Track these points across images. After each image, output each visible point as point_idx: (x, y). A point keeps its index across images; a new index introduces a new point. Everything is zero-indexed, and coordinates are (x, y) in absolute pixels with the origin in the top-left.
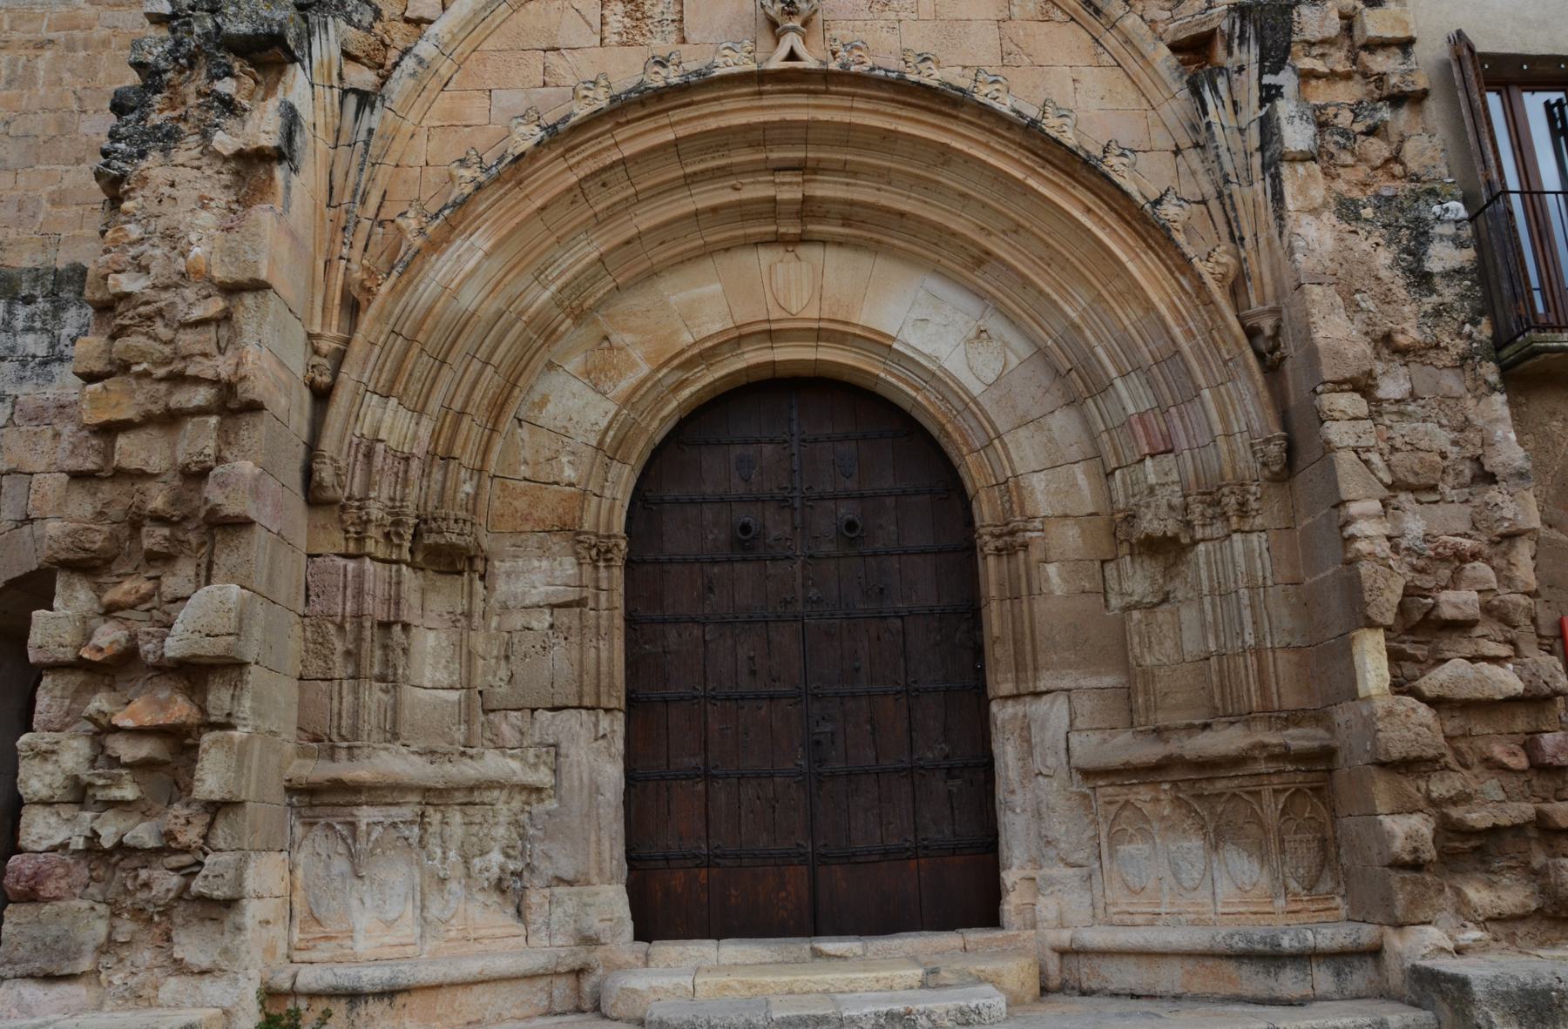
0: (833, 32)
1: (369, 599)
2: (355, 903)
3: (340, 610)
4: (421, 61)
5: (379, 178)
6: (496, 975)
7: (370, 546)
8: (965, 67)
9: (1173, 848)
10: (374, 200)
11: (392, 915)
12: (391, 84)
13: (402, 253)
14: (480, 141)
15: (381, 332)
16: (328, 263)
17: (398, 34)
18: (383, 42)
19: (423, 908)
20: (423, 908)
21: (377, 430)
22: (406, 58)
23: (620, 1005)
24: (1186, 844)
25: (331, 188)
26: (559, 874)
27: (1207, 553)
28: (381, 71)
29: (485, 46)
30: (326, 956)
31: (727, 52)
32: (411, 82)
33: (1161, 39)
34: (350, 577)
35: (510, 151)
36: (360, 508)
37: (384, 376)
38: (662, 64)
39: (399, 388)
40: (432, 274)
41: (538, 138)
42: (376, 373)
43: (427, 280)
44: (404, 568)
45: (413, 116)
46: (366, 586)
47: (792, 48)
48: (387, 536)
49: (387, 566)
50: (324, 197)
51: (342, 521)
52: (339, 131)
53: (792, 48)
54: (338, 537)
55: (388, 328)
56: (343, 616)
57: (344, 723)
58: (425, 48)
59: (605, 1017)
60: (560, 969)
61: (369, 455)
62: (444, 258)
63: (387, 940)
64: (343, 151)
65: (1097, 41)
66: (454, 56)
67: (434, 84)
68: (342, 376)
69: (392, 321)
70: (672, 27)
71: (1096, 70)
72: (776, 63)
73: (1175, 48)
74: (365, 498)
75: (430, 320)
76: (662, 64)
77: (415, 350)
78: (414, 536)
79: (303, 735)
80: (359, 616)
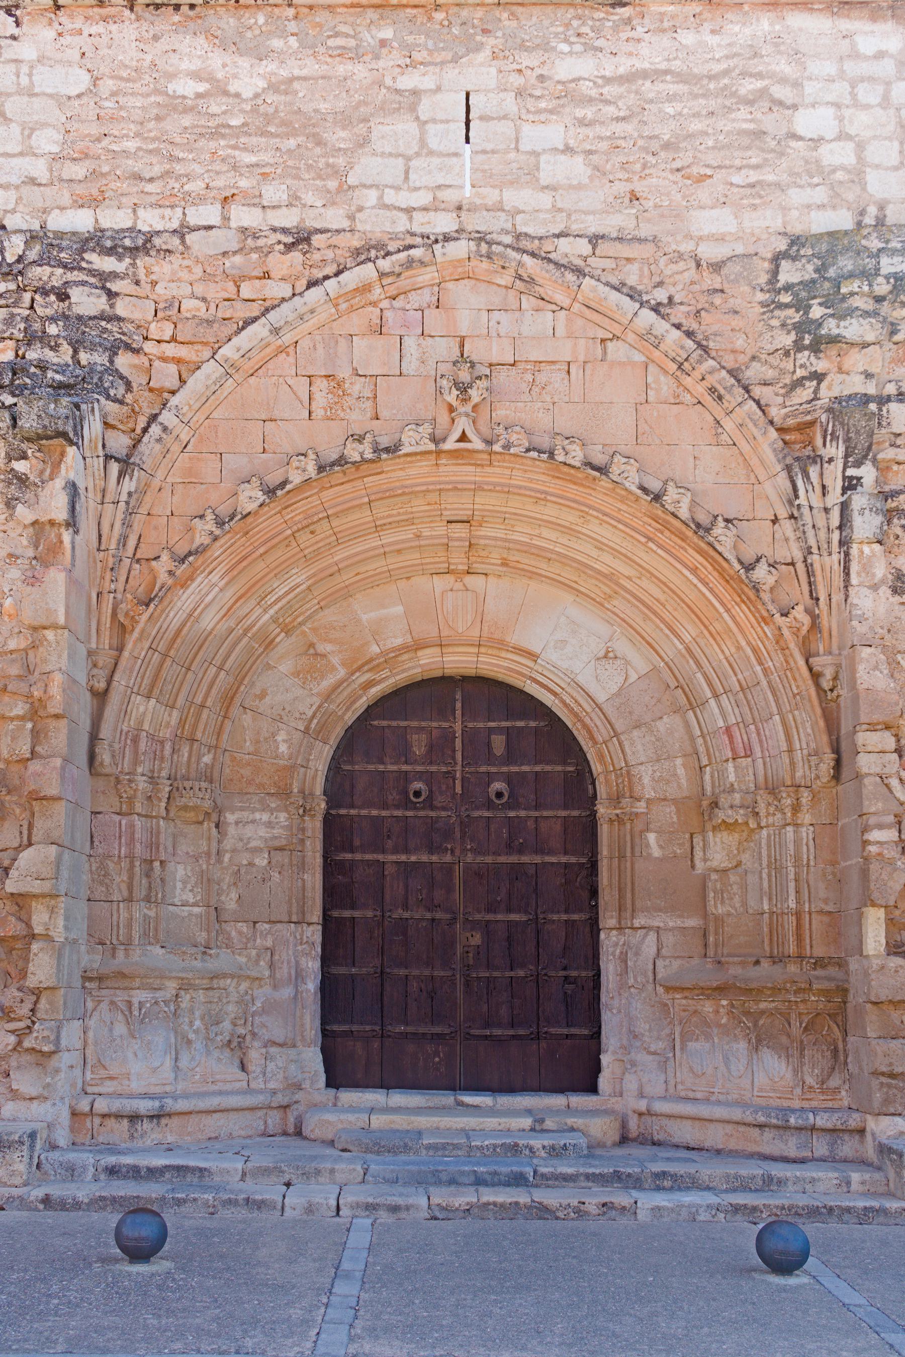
0: (498, 412)
1: (138, 845)
2: (130, 1055)
3: (116, 852)
4: (165, 429)
5: (135, 525)
6: (229, 1107)
7: (138, 808)
8: (604, 445)
9: (726, 1047)
10: (132, 543)
11: (157, 1064)
12: (142, 447)
13: (157, 589)
14: (214, 498)
15: (142, 649)
16: (99, 594)
17: (146, 405)
18: (133, 410)
19: (176, 1059)
20: (176, 1059)
21: (141, 722)
22: (153, 426)
23: (317, 1130)
24: (735, 1046)
25: (100, 536)
26: (273, 1039)
27: (769, 836)
28: (132, 435)
29: (215, 415)
30: (111, 1090)
31: (411, 433)
32: (158, 447)
33: (771, 422)
34: (123, 829)
35: (239, 510)
36: (130, 781)
37: (145, 682)
38: (360, 439)
39: (156, 691)
40: (179, 604)
41: (261, 500)
42: (139, 679)
43: (176, 609)
44: (162, 822)
45: (160, 475)
46: (136, 836)
47: (464, 432)
48: (149, 798)
49: (149, 820)
50: (96, 545)
51: (117, 790)
52: (104, 490)
53: (464, 432)
54: (115, 801)
55: (147, 645)
56: (119, 857)
57: (121, 932)
58: (167, 417)
59: (306, 1138)
60: (273, 1105)
61: (136, 740)
62: (189, 591)
63: (153, 1080)
64: (109, 508)
65: (718, 422)
66: (191, 424)
67: (176, 448)
68: (114, 684)
69: (150, 640)
70: (369, 404)
71: (714, 448)
72: (450, 444)
73: (780, 430)
74: (132, 773)
75: (179, 641)
76: (360, 439)
77: (169, 662)
78: (169, 798)
79: (91, 939)
80: (131, 857)
